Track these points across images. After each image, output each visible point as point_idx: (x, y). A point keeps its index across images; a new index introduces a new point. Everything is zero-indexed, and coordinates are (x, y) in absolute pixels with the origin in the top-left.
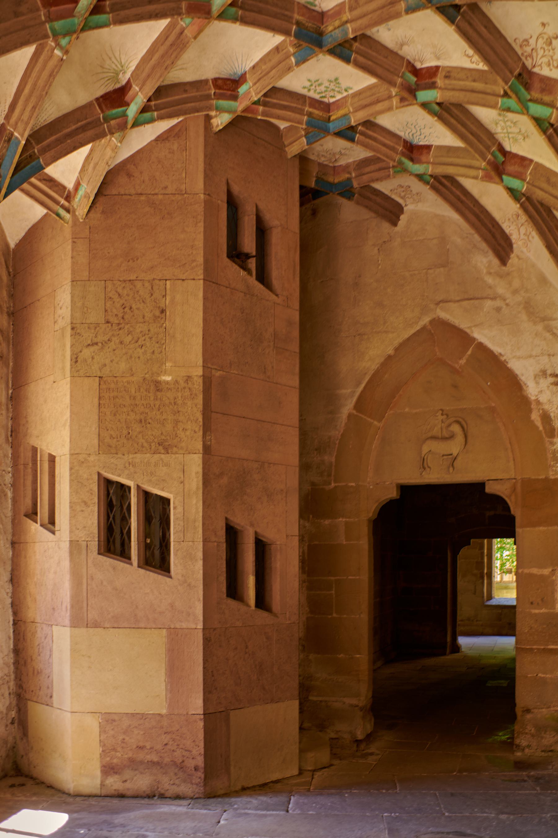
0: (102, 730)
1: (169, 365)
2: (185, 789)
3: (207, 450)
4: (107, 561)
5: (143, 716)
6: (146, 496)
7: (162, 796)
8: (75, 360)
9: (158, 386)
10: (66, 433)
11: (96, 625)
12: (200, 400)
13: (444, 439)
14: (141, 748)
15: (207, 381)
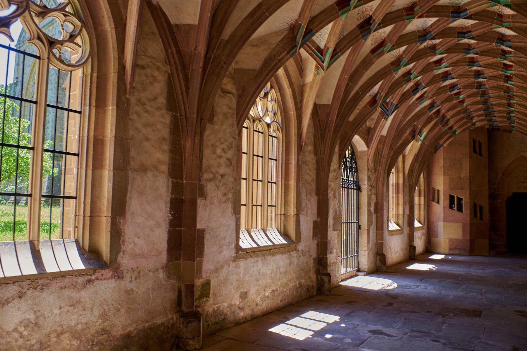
0: (449, 242)
1: (463, 174)
2: (465, 254)
3: (470, 189)
4: (450, 210)
5: (457, 239)
6: (458, 198)
7: (461, 255)
8: (444, 173)
9: (461, 178)
10: (442, 186)
11: (448, 222)
12: (469, 180)
13: (524, 182)
14: (457, 245)
15: (470, 177)
